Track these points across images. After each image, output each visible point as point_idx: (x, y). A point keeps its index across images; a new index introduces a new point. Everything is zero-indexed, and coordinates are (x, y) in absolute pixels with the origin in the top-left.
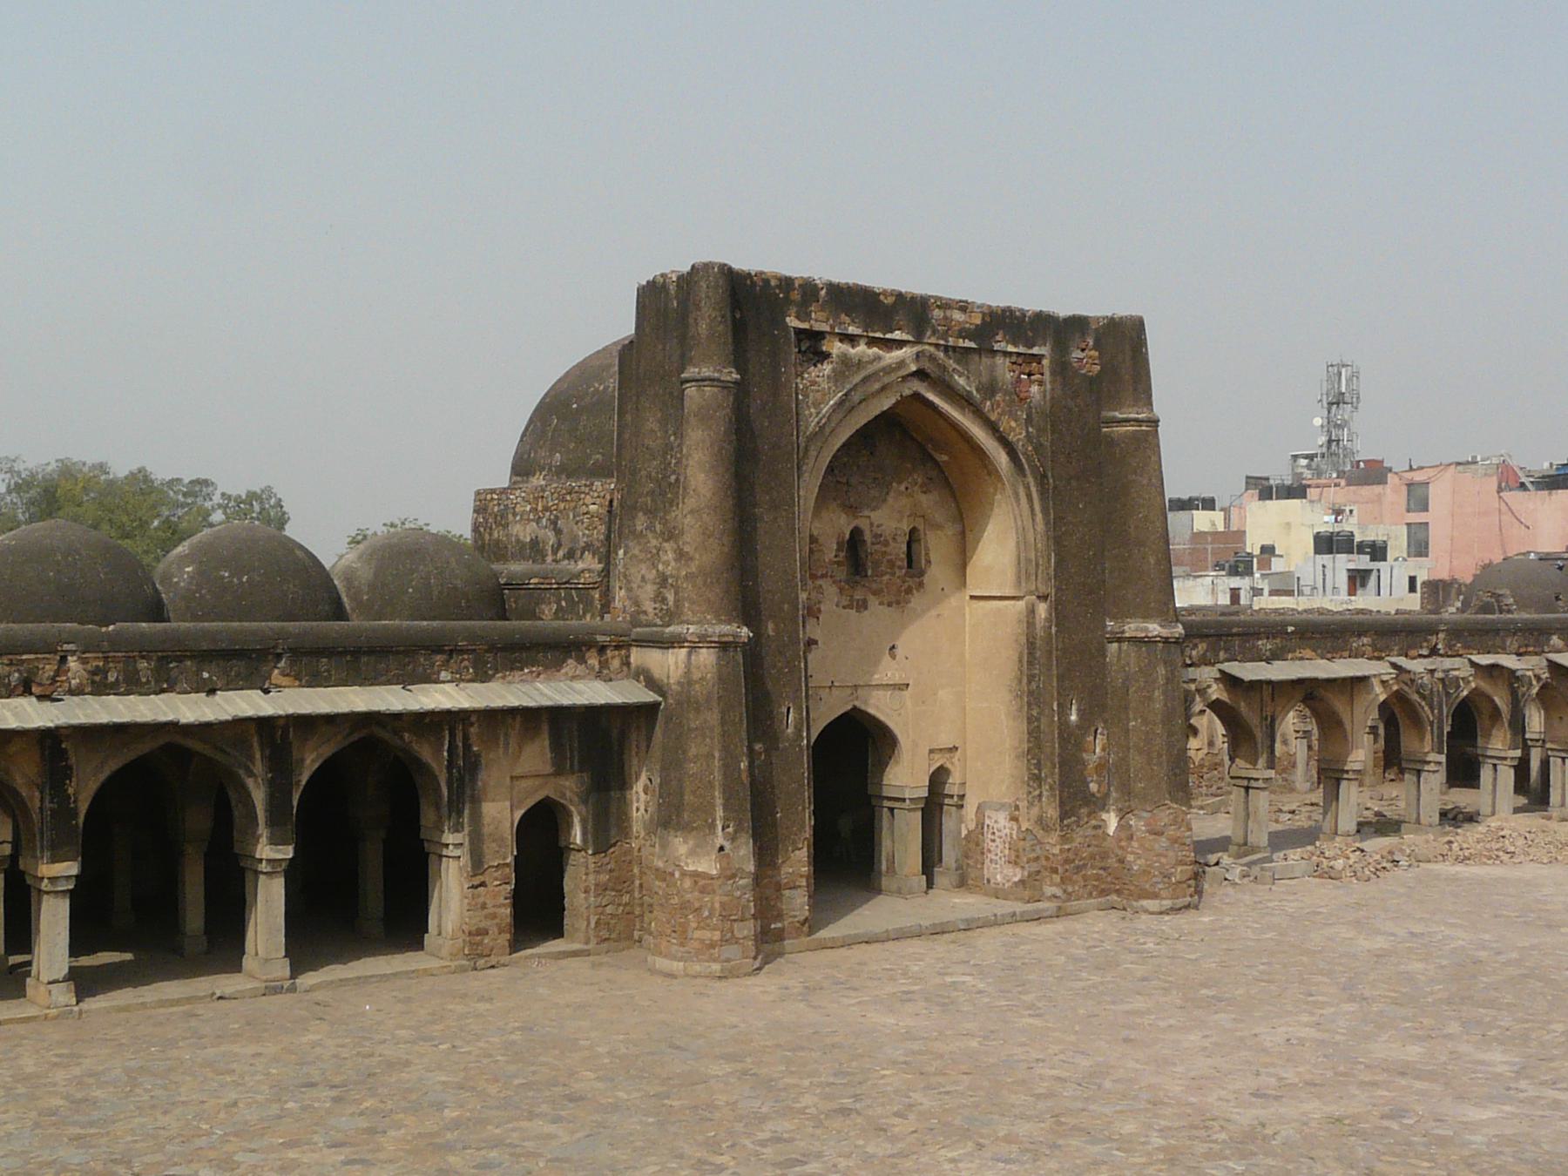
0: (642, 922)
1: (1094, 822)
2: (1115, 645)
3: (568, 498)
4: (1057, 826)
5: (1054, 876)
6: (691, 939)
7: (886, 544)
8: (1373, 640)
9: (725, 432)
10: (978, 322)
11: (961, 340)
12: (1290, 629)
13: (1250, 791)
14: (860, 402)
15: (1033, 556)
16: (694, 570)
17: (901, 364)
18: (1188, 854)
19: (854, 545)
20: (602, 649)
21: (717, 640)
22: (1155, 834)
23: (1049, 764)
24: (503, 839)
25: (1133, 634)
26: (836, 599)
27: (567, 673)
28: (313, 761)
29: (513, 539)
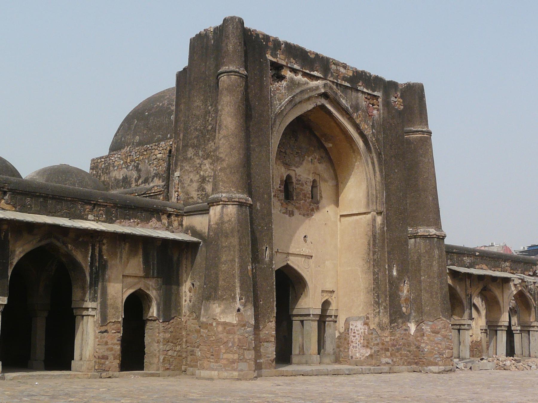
0: (187, 361)
1: (404, 327)
2: (413, 240)
3: (145, 153)
4: (388, 327)
5: (387, 352)
6: (222, 359)
7: (302, 185)
8: (511, 265)
9: (241, 99)
10: (351, 74)
11: (344, 82)
12: (477, 254)
13: (461, 331)
14: (299, 103)
15: (375, 193)
16: (225, 166)
17: (317, 88)
19: (287, 183)
20: (169, 216)
22: (436, 333)
23: (383, 296)
24: (117, 308)
25: (423, 234)
27: (151, 225)
28: (20, 252)
29: (113, 179)
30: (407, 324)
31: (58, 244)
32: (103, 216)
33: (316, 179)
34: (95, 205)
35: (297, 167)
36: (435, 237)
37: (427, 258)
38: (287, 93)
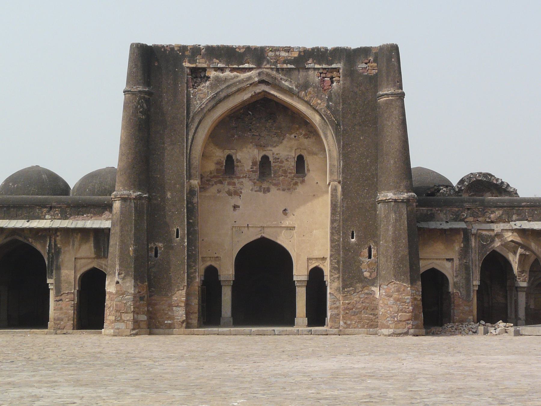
1: (366, 291)
2: (379, 205)
15: (336, 163)
17: (250, 78)
18: (407, 307)
21: (119, 196)
24: (70, 282)
26: (251, 188)
30: (371, 288)
31: (21, 239)
32: (58, 215)
33: (303, 154)
34: (51, 208)
35: (275, 147)
36: (392, 202)
37: (385, 223)
38: (210, 91)
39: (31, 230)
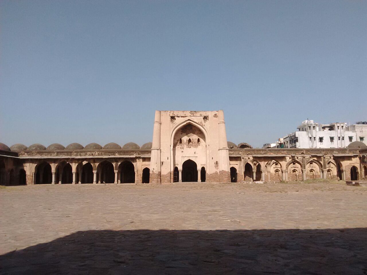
19: (190, 141)
39: (130, 158)
